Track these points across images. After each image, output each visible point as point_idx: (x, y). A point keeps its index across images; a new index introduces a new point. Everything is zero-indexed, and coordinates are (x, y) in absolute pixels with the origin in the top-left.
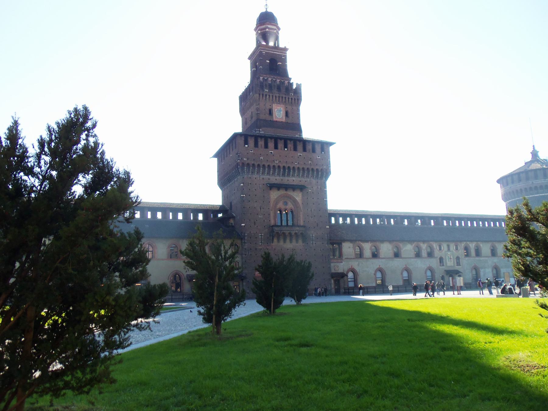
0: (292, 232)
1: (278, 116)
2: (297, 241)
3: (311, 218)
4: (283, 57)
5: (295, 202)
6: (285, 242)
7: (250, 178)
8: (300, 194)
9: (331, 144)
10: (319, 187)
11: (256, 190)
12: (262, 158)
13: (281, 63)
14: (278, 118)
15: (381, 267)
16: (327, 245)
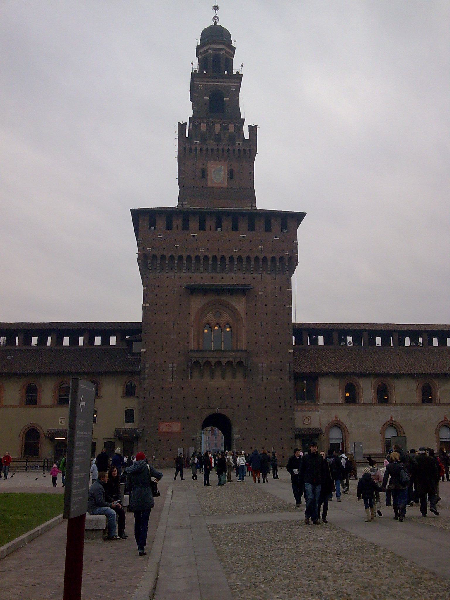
0: (222, 360)
1: (215, 180)
2: (234, 377)
3: (260, 337)
4: (233, 88)
5: (234, 312)
6: (212, 376)
7: (158, 277)
8: (243, 300)
9: (299, 217)
10: (277, 286)
11: (167, 295)
12: (178, 245)
13: (229, 99)
14: (215, 182)
15: (394, 419)
16: (288, 381)
